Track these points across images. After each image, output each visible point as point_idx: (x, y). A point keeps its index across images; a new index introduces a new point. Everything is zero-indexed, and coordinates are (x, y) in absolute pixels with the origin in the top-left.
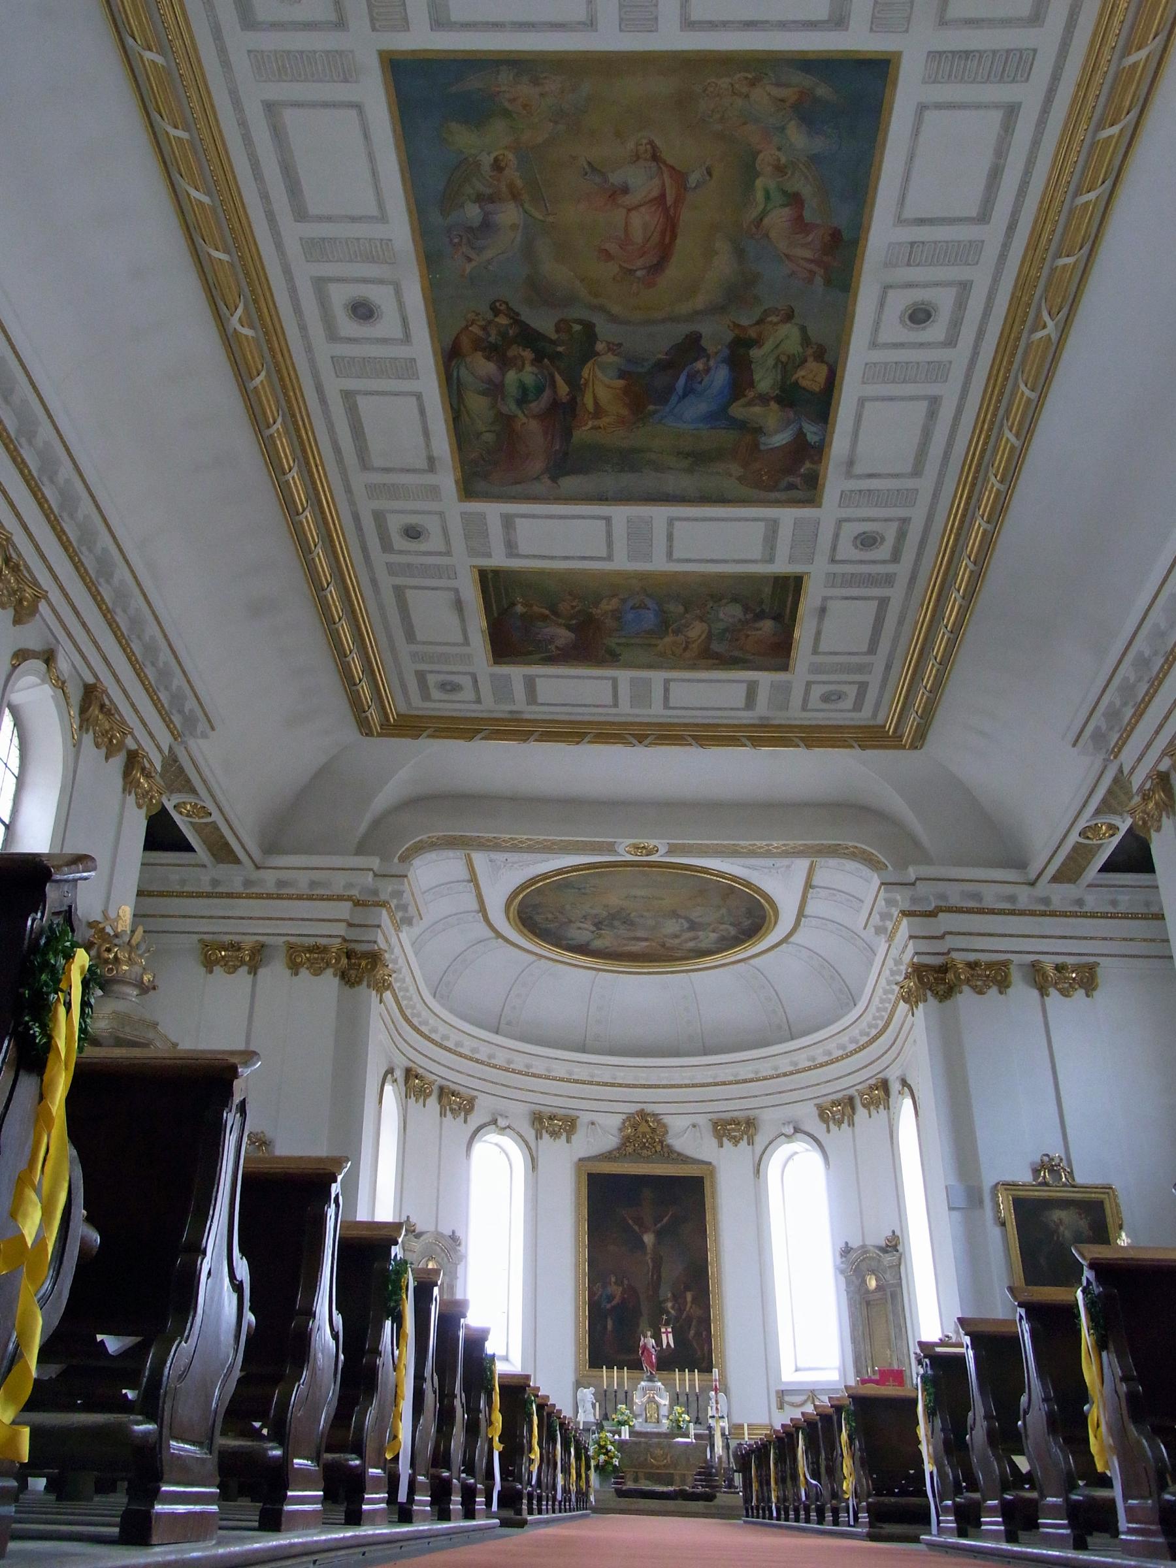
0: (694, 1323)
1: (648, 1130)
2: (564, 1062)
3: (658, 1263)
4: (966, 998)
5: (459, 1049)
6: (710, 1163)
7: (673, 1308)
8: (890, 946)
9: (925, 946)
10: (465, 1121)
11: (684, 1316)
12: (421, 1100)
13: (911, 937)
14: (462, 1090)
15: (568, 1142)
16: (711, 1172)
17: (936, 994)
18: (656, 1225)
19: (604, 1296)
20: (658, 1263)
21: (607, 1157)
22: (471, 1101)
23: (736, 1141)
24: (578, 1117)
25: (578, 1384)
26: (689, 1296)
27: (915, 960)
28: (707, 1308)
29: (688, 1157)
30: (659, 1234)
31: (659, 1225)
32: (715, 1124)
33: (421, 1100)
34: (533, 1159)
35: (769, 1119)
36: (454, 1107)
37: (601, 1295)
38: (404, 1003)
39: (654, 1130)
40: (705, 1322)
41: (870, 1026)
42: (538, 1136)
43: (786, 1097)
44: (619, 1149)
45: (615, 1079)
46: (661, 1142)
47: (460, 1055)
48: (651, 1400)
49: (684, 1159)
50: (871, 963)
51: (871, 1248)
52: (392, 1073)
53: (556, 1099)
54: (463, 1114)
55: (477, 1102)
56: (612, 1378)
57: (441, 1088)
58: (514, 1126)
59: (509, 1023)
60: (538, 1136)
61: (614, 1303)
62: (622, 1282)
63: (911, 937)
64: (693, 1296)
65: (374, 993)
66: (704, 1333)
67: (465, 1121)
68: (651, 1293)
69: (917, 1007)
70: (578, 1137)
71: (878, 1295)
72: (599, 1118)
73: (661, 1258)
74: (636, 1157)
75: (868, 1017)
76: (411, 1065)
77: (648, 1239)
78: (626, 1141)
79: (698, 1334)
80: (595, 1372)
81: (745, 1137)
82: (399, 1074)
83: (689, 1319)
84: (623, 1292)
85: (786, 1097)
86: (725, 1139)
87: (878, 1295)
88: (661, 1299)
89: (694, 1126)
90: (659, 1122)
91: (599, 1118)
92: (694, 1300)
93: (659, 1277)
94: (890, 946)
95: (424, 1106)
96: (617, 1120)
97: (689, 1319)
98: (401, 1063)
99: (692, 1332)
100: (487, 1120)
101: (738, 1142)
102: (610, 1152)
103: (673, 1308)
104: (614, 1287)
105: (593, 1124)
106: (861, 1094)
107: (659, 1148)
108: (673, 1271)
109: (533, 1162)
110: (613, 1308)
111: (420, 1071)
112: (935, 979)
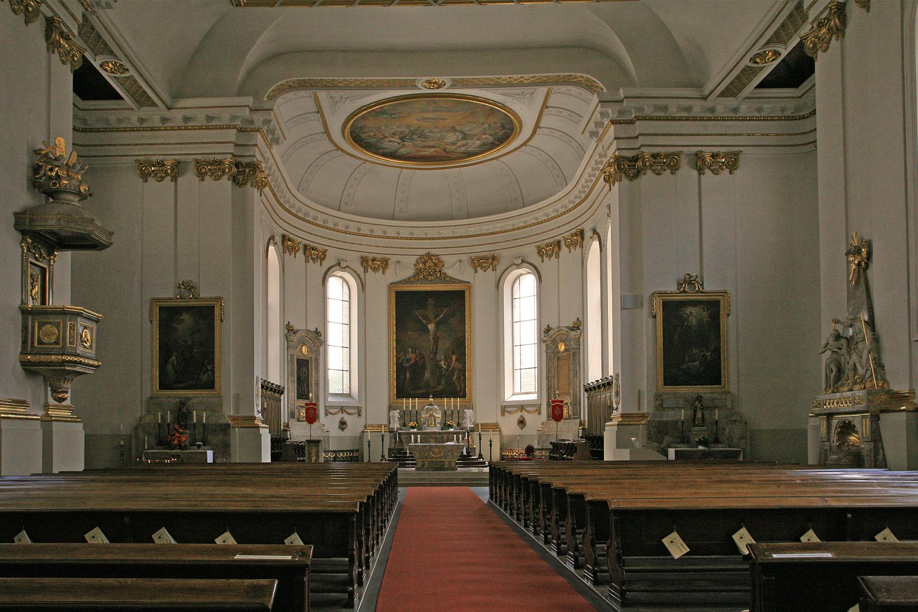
0: (456, 372)
1: (433, 265)
2: (380, 225)
4: (648, 177)
5: (315, 221)
6: (469, 283)
7: (444, 364)
8: (598, 144)
9: (624, 144)
11: (451, 369)
12: (293, 254)
13: (615, 138)
15: (383, 274)
17: (628, 176)
18: (435, 319)
21: (407, 281)
22: (324, 252)
23: (485, 269)
24: (390, 259)
25: (390, 408)
26: (454, 357)
27: (617, 153)
29: (456, 279)
30: (438, 325)
32: (473, 261)
33: (293, 254)
34: (362, 284)
35: (505, 256)
37: (403, 359)
38: (278, 195)
39: (436, 265)
41: (576, 197)
42: (366, 271)
43: (520, 242)
44: (414, 276)
45: (412, 235)
46: (440, 271)
47: (316, 225)
48: (431, 415)
49: (453, 281)
50: (581, 158)
51: (563, 328)
52: (273, 239)
53: (375, 249)
55: (327, 253)
56: (409, 403)
57: (305, 246)
59: (346, 204)
60: (366, 271)
61: (411, 363)
62: (416, 352)
63: (615, 138)
65: (256, 190)
66: (462, 377)
68: (432, 357)
69: (614, 185)
70: (390, 271)
71: (565, 354)
72: (404, 259)
74: (425, 280)
75: (576, 192)
76: (285, 233)
78: (419, 272)
79: (458, 378)
80: (400, 401)
82: (278, 239)
83: (453, 371)
84: (416, 357)
85: (520, 242)
86: (479, 269)
87: (565, 354)
89: (460, 261)
90: (439, 259)
91: (404, 259)
92: (457, 360)
93: (437, 348)
94: (598, 144)
95: (295, 257)
96: (413, 260)
97: (453, 371)
98: (278, 232)
99: (455, 377)
100: (334, 263)
102: (409, 278)
103: (444, 364)
104: (411, 355)
105: (399, 262)
106: (566, 239)
107: (438, 275)
108: (445, 344)
109: (362, 286)
110: (411, 366)
111: (291, 236)
112: (628, 166)
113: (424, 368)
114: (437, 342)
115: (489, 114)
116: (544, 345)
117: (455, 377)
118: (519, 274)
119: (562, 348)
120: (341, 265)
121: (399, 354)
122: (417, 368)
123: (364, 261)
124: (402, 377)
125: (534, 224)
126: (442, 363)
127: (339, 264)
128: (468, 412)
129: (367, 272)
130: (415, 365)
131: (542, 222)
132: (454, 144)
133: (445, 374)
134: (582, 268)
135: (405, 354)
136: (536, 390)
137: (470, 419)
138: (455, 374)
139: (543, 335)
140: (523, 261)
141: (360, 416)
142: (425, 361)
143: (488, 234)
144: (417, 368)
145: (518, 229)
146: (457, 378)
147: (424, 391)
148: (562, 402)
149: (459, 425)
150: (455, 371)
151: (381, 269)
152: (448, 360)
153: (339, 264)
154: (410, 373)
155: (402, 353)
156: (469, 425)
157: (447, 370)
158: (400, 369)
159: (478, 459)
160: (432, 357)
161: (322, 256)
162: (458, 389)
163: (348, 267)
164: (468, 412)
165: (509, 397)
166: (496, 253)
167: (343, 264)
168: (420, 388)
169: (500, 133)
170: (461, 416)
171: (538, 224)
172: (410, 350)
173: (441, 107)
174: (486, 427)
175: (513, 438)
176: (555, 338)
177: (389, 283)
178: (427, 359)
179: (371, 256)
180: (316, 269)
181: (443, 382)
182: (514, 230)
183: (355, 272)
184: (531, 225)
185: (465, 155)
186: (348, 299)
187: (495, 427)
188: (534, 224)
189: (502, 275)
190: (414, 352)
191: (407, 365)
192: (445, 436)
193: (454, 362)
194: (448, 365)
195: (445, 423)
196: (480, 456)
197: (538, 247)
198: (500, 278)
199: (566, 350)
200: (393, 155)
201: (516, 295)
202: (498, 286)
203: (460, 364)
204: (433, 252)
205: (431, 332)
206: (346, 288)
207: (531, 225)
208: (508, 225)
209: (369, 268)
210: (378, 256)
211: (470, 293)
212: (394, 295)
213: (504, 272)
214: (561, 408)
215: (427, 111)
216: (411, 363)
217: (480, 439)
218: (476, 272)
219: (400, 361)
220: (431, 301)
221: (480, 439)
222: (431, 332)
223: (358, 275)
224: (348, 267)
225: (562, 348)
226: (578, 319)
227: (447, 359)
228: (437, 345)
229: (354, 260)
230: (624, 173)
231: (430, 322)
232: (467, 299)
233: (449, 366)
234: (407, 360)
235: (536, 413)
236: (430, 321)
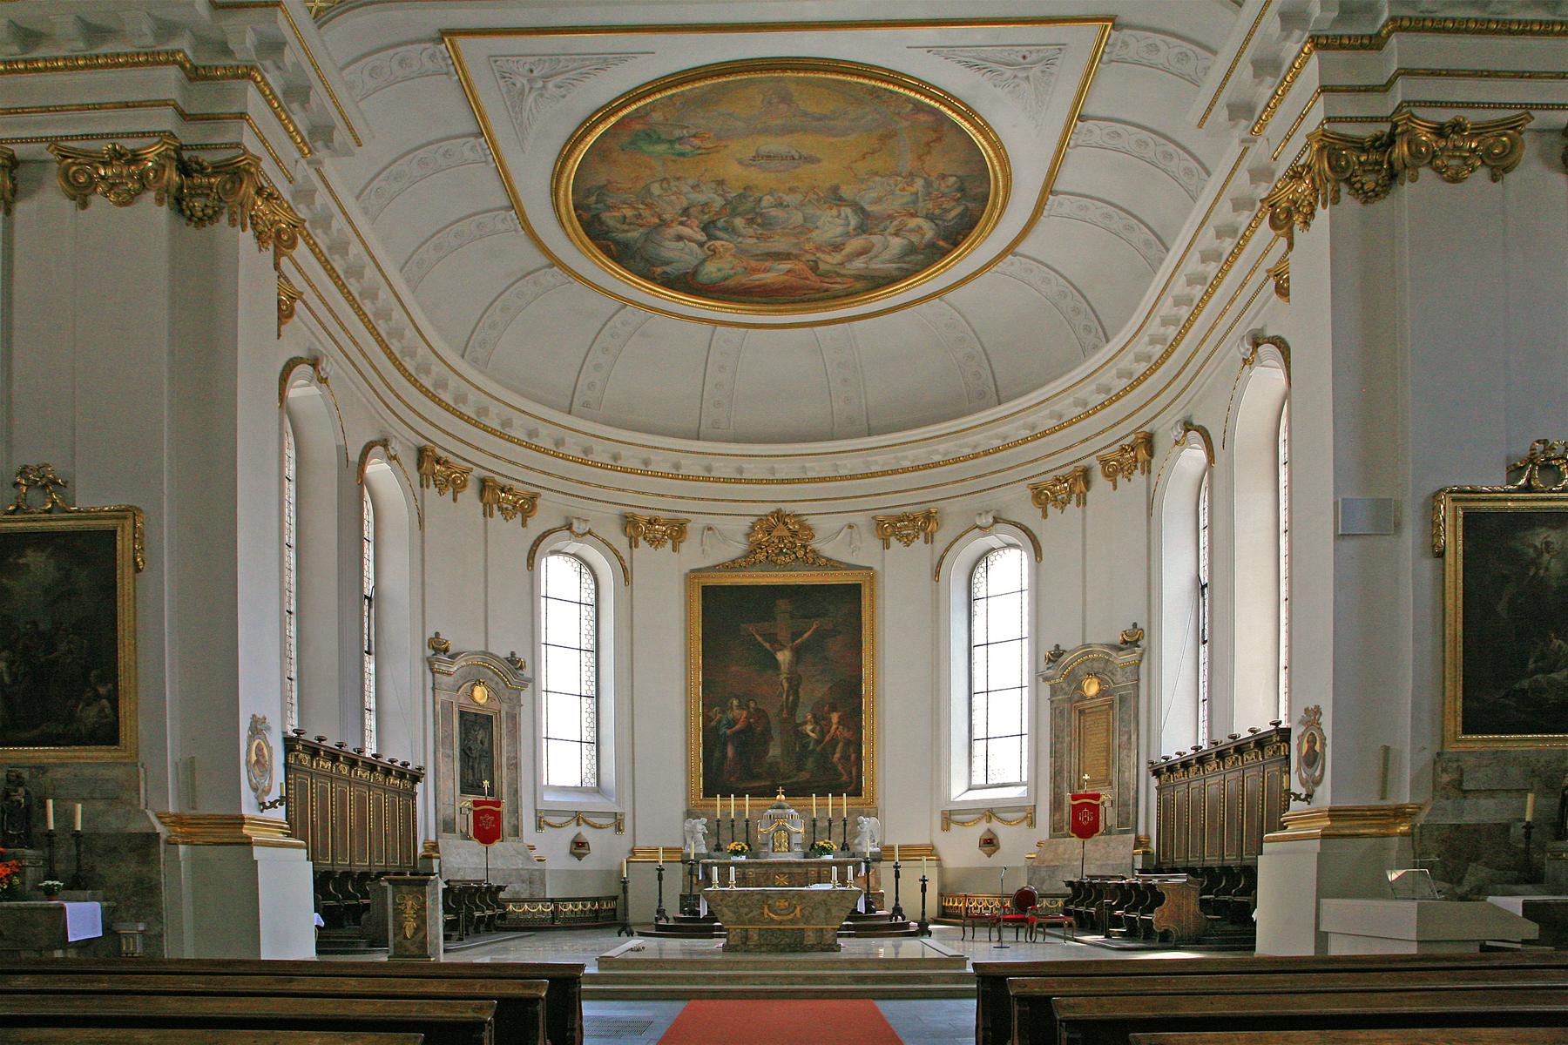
0: (840, 745)
3: (795, 683)
6: (871, 568)
10: (524, 524)
11: (827, 738)
14: (515, 485)
16: (872, 577)
20: (795, 683)
22: (532, 499)
26: (835, 717)
30: (797, 653)
31: (799, 641)
32: (879, 524)
34: (624, 569)
36: (505, 506)
37: (720, 721)
40: (855, 742)
54: (519, 515)
55: (538, 501)
58: (594, 530)
61: (737, 727)
62: (749, 707)
64: (839, 717)
66: (853, 756)
67: (524, 524)
77: (784, 657)
79: (845, 757)
81: (922, 535)
83: (834, 742)
86: (893, 539)
88: (798, 721)
97: (834, 742)
99: (837, 756)
104: (737, 712)
108: (815, 690)
113: (766, 736)
115: (928, 144)
116: (1045, 689)
117: (837, 756)
118: (987, 548)
119: (1092, 688)
120: (575, 527)
121: (710, 709)
122: (751, 739)
123: (629, 523)
124: (717, 754)
125: (1026, 441)
126: (809, 728)
127: (569, 527)
128: (868, 823)
129: (636, 546)
130: (748, 729)
131: (1044, 434)
132: (837, 248)
133: (813, 751)
134: (1150, 515)
136: (1025, 779)
137: (872, 836)
138: (838, 750)
139: (1043, 665)
140: (996, 520)
141: (620, 830)
143: (916, 469)
144: (751, 739)
145: (987, 453)
146: (842, 757)
147: (768, 783)
148: (1097, 797)
149: (845, 847)
150: (838, 743)
151: (670, 542)
152: (823, 723)
153: (569, 527)
156: (869, 848)
157: (818, 742)
158: (712, 740)
159: (890, 917)
161: (527, 507)
162: (844, 778)
163: (590, 532)
164: (868, 823)
165: (958, 792)
166: (933, 507)
167: (578, 527)
168: (758, 777)
169: (953, 213)
170: (849, 829)
171: (1035, 438)
172: (735, 702)
173: (805, 114)
174: (909, 852)
175: (970, 874)
176: (1073, 668)
177: (687, 571)
179: (646, 514)
180: (510, 534)
181: (810, 764)
182: (976, 456)
183: (608, 545)
184: (1016, 444)
185: (859, 285)
186: (593, 602)
187: (930, 851)
188: (1026, 441)
189: (947, 550)
191: (728, 732)
192: (813, 871)
193: (834, 727)
194: (822, 730)
195: (813, 845)
196: (897, 910)
197: (1035, 487)
198: (942, 558)
199: (1102, 693)
200: (687, 283)
201: (979, 591)
202: (937, 573)
204: (788, 508)
205: (784, 667)
206: (588, 579)
207: (1016, 444)
208: (963, 446)
209: (640, 538)
210: (663, 515)
211: (872, 590)
212: (698, 595)
213: (951, 545)
214: (1095, 809)
215: (766, 131)
216: (737, 727)
217: (897, 876)
218: (887, 546)
219: (713, 724)
220: (783, 605)
221: (897, 876)
222: (784, 667)
223: (616, 553)
224: (590, 532)
225: (1092, 688)
226: (1135, 625)
227: (820, 720)
228: (796, 693)
229: (607, 521)
230: (1347, 181)
231: (783, 647)
232: (865, 603)
233: (823, 733)
234: (729, 721)
235: (1025, 823)
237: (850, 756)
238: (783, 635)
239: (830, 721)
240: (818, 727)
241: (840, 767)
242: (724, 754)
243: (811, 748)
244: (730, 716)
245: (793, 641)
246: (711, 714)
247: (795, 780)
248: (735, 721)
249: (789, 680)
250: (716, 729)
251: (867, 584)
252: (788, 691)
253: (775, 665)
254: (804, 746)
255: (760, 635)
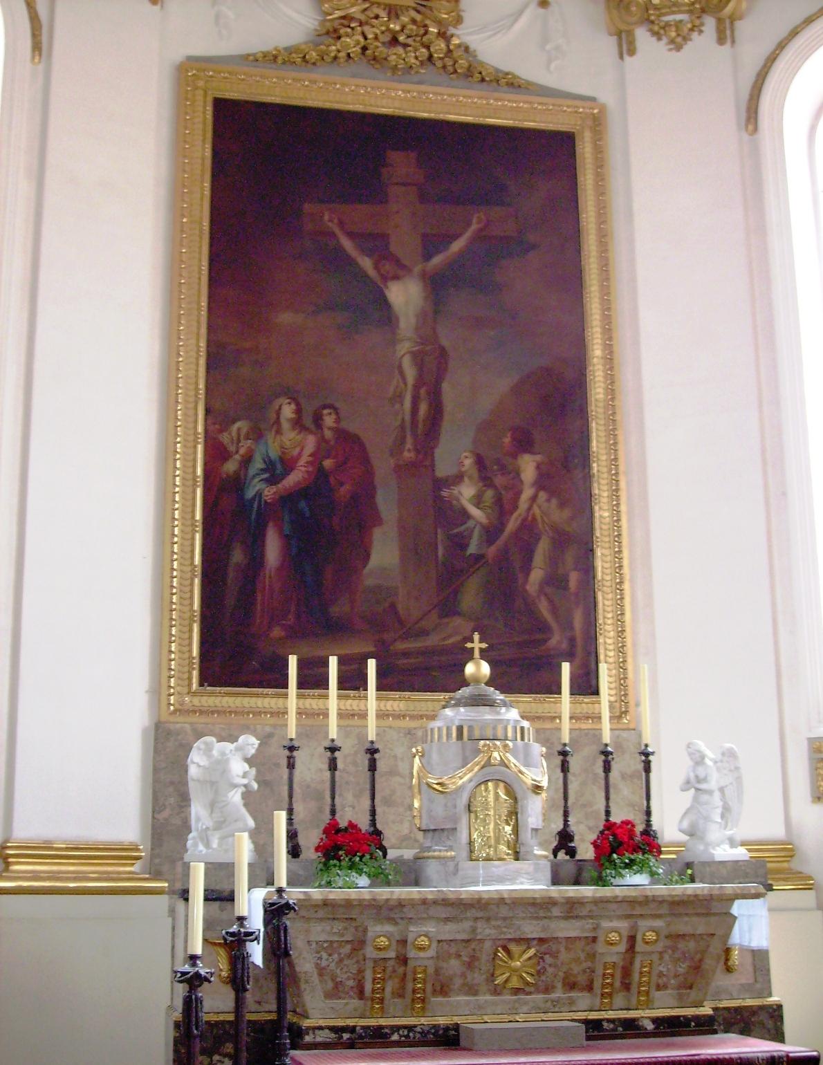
11: (512, 524)
19: (258, 464)
26: (528, 466)
28: (583, 505)
31: (437, 260)
37: (247, 460)
62: (318, 419)
64: (538, 467)
68: (408, 455)
73: (443, 354)
79: (555, 581)
83: (528, 534)
92: (544, 481)
97: (528, 534)
99: (536, 575)
101: (686, 39)
103: (478, 501)
104: (290, 436)
110: (288, 499)
114: (439, 380)
124: (237, 556)
133: (478, 558)
135: (257, 434)
142: (369, 473)
152: (499, 480)
154: (286, 539)
155: (241, 425)
157: (491, 533)
160: (408, 455)
172: (288, 411)
178: (383, 465)
190: (307, 422)
191: (269, 493)
194: (499, 501)
203: (562, 505)
218: (627, 46)
219: (231, 467)
231: (400, 270)
233: (503, 508)
234: (270, 466)
236: (403, 267)
237: (566, 580)
238: (404, 242)
239: (518, 474)
240: (490, 493)
241: (544, 608)
242: (256, 560)
243: (472, 549)
244: (272, 447)
245: (428, 257)
246: (225, 438)
247: (432, 641)
248: (288, 464)
249: (419, 358)
250: (237, 484)
251: (588, 135)
252: (417, 387)
253: (385, 315)
254: (459, 543)
255: (351, 235)
